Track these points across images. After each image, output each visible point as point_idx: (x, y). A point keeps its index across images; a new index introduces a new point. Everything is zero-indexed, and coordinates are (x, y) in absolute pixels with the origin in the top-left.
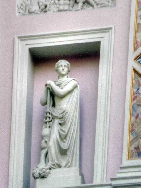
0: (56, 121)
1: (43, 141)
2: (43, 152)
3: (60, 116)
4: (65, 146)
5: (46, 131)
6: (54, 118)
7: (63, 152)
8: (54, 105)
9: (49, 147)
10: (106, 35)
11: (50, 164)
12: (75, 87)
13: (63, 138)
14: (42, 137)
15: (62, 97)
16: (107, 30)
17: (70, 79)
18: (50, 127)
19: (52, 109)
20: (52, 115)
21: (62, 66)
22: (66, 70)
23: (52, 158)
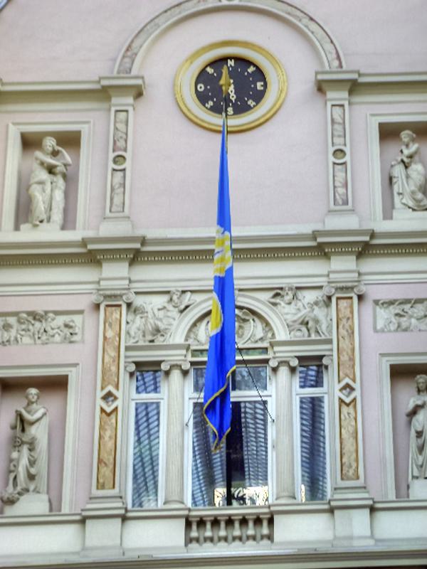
0: (25, 449)
1: (12, 465)
2: (12, 476)
3: (30, 441)
4: (33, 471)
5: (15, 455)
6: (23, 443)
7: (31, 477)
8: (23, 430)
9: (18, 472)
10: (73, 369)
11: (19, 489)
12: (44, 414)
13: (32, 463)
14: (11, 460)
15: (32, 423)
16: (75, 365)
17: (39, 407)
18: (19, 451)
19: (21, 434)
20: (21, 440)
21: (32, 394)
22: (36, 397)
23: (21, 481)
